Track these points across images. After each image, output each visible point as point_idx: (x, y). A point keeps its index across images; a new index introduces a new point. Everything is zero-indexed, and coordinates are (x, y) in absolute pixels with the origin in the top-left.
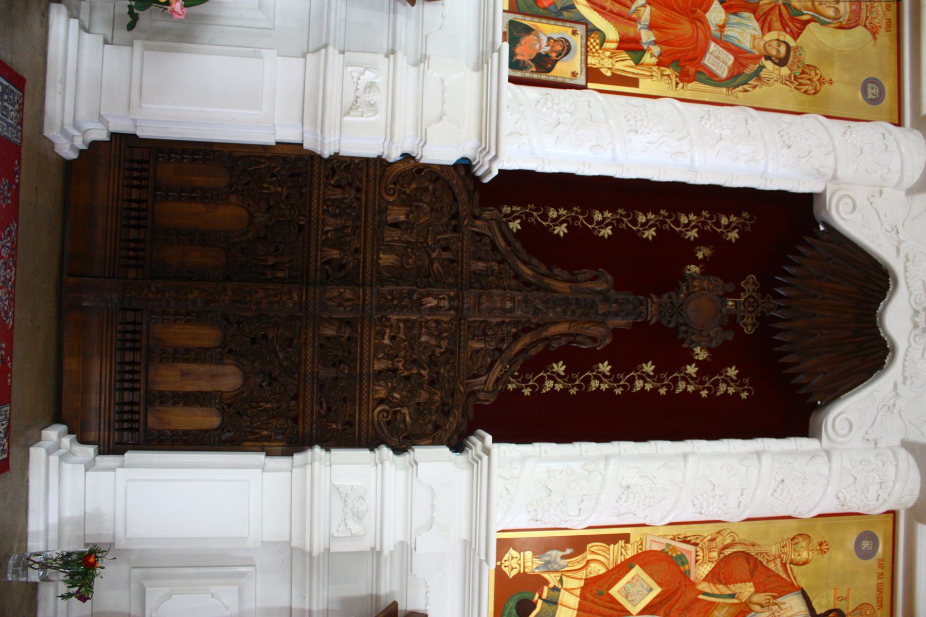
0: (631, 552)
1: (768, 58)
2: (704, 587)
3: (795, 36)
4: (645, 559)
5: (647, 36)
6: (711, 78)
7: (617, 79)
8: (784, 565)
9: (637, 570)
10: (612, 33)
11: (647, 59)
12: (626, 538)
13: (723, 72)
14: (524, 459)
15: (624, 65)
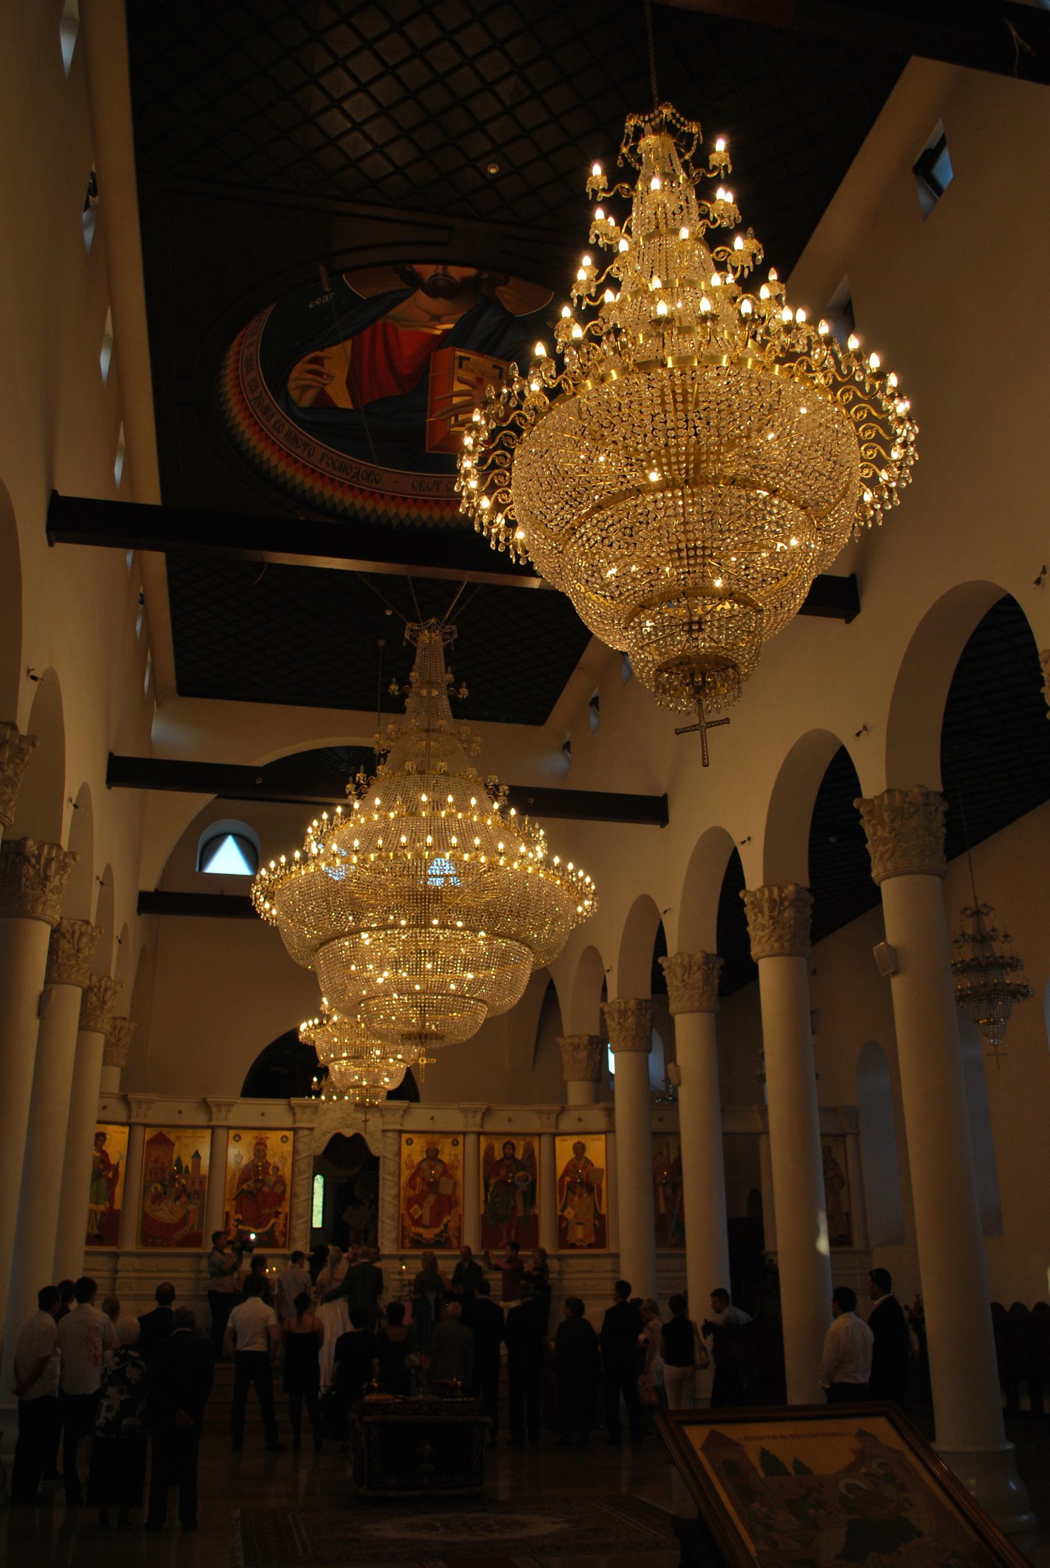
0: (406, 1213)
1: (277, 1173)
2: (417, 1192)
3: (270, 1164)
4: (408, 1209)
5: (274, 1210)
6: (284, 1191)
7: (286, 1219)
8: (413, 1168)
9: (411, 1211)
10: (273, 1220)
11: (280, 1210)
12: (402, 1214)
13: (282, 1188)
14: (382, 1243)
15: (282, 1216)
